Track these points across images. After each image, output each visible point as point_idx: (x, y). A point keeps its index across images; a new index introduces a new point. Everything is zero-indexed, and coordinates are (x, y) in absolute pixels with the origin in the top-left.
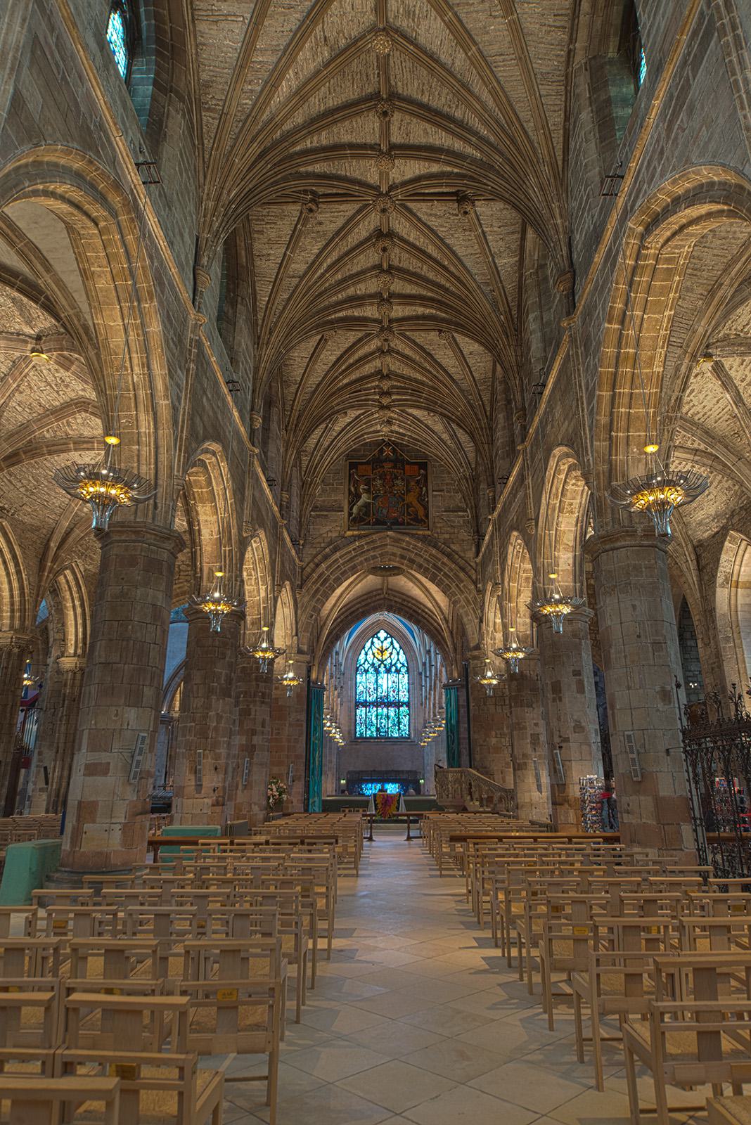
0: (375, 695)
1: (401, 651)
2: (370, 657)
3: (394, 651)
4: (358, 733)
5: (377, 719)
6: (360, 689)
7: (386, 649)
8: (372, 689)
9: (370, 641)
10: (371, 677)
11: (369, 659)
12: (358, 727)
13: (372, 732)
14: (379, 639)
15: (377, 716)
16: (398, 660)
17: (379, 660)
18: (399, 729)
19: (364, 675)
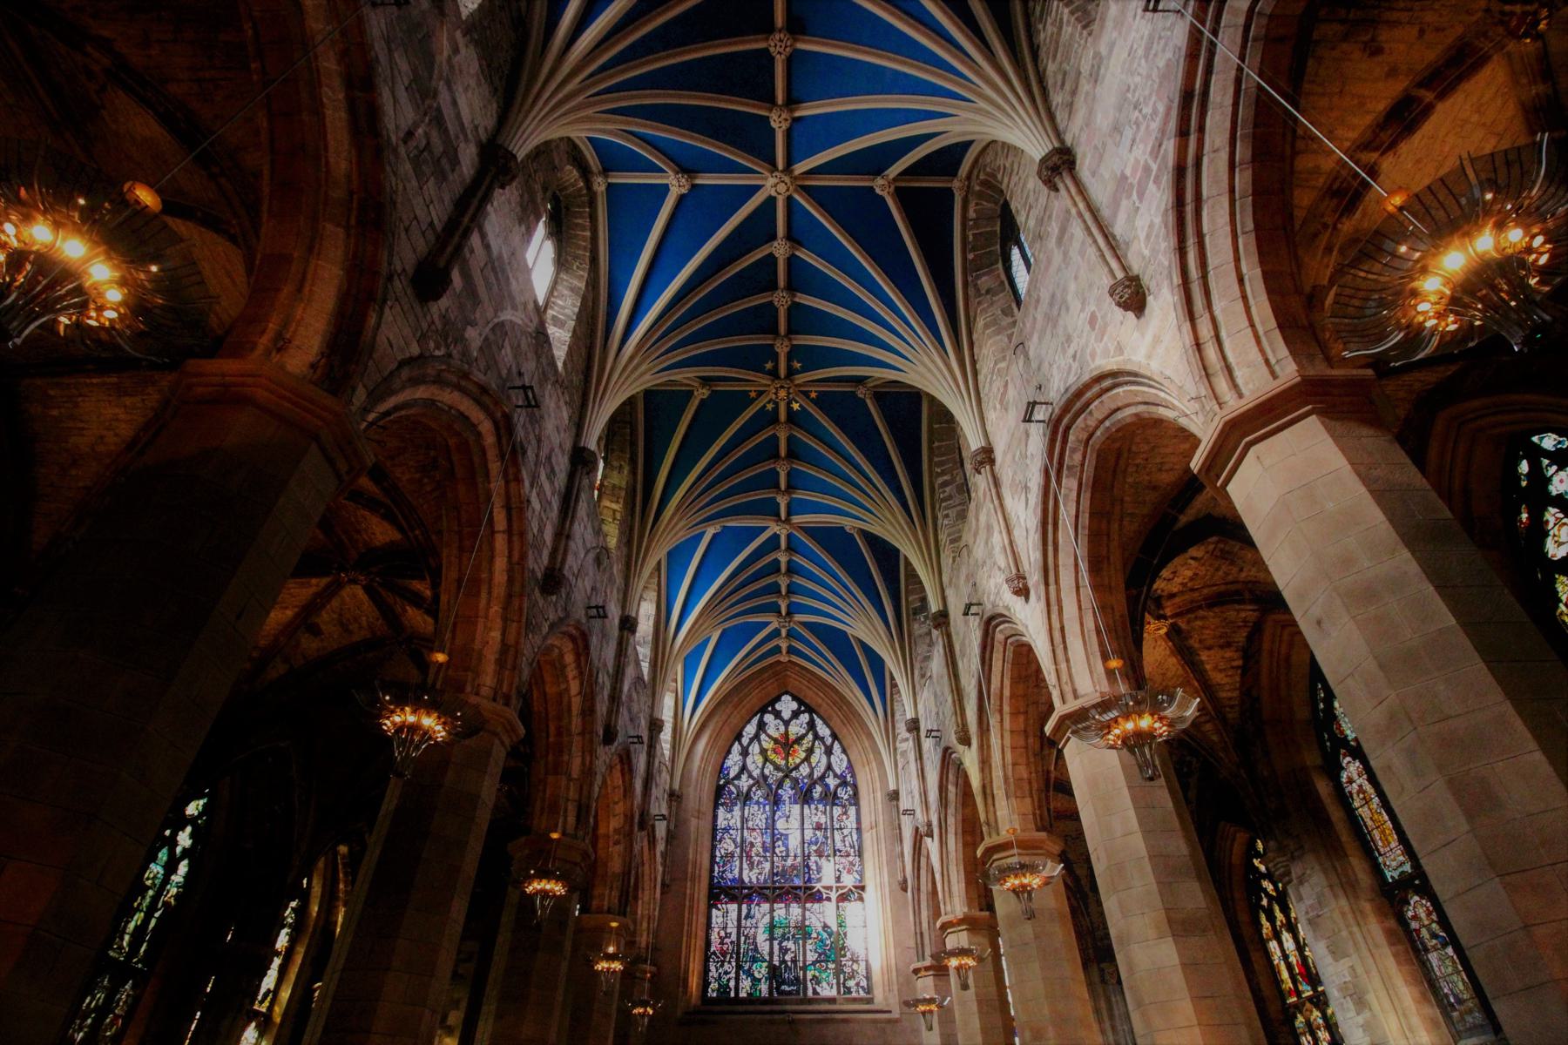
0: (767, 866)
1: (837, 746)
2: (755, 761)
3: (819, 751)
4: (714, 985)
5: (771, 939)
6: (727, 846)
7: (799, 740)
8: (758, 848)
9: (755, 721)
10: (758, 815)
11: (751, 766)
12: (713, 968)
13: (755, 981)
14: (778, 715)
15: (772, 927)
16: (829, 767)
17: (777, 768)
18: (839, 971)
19: (737, 810)
